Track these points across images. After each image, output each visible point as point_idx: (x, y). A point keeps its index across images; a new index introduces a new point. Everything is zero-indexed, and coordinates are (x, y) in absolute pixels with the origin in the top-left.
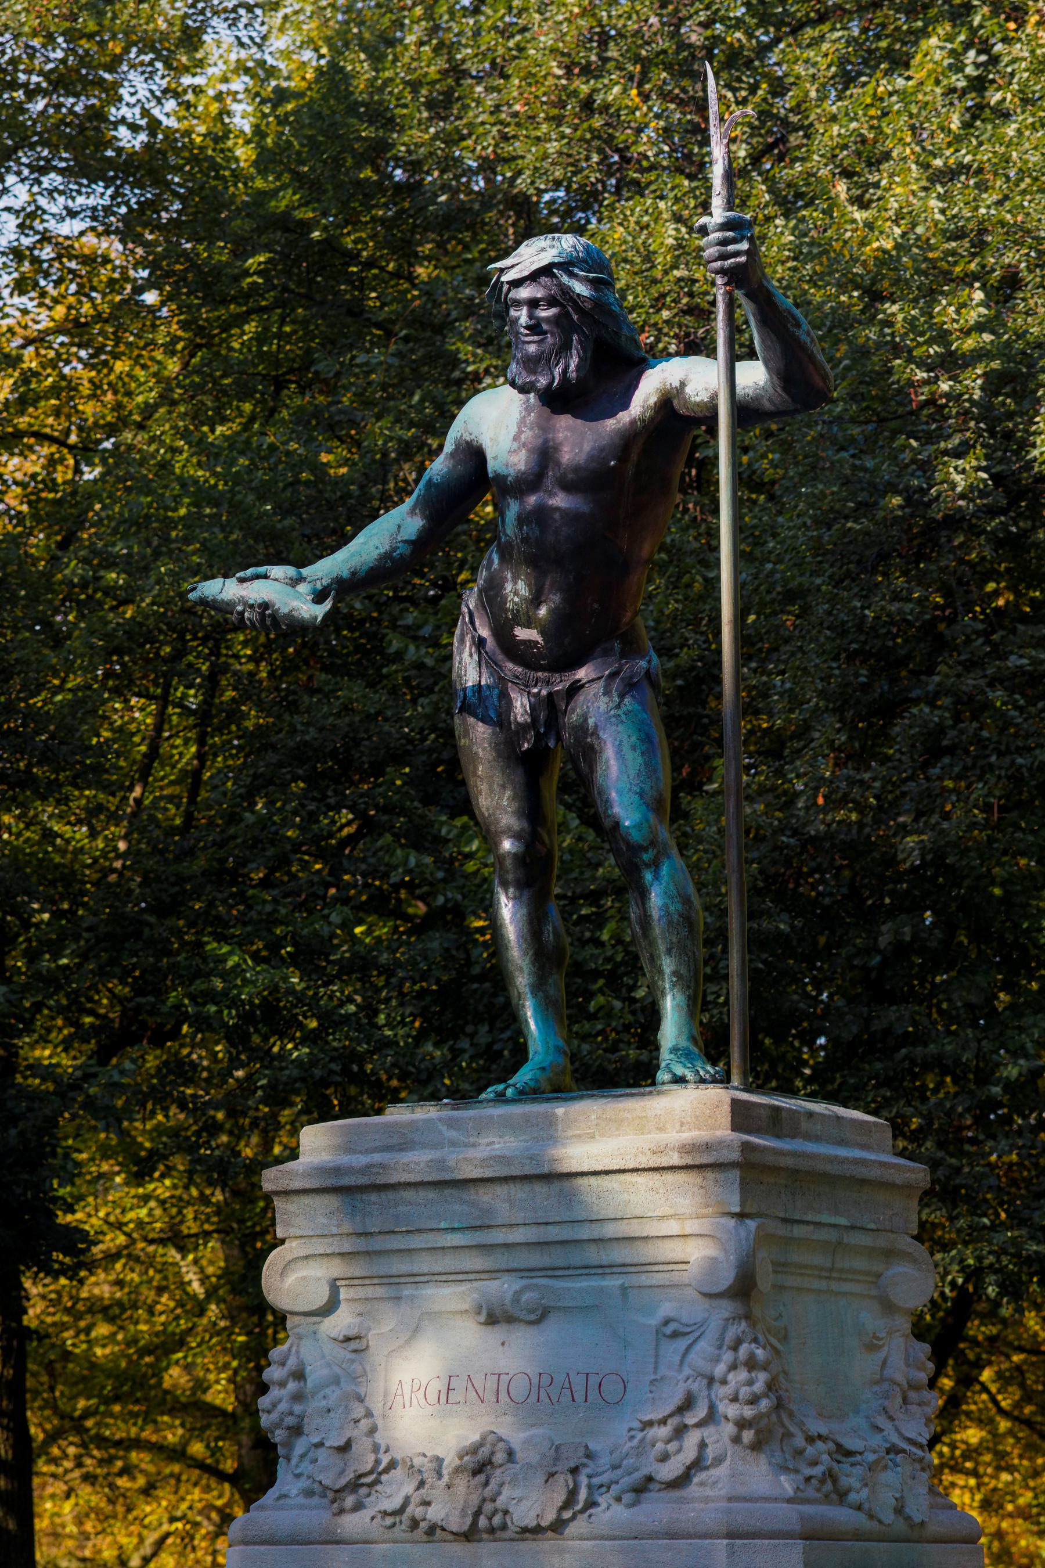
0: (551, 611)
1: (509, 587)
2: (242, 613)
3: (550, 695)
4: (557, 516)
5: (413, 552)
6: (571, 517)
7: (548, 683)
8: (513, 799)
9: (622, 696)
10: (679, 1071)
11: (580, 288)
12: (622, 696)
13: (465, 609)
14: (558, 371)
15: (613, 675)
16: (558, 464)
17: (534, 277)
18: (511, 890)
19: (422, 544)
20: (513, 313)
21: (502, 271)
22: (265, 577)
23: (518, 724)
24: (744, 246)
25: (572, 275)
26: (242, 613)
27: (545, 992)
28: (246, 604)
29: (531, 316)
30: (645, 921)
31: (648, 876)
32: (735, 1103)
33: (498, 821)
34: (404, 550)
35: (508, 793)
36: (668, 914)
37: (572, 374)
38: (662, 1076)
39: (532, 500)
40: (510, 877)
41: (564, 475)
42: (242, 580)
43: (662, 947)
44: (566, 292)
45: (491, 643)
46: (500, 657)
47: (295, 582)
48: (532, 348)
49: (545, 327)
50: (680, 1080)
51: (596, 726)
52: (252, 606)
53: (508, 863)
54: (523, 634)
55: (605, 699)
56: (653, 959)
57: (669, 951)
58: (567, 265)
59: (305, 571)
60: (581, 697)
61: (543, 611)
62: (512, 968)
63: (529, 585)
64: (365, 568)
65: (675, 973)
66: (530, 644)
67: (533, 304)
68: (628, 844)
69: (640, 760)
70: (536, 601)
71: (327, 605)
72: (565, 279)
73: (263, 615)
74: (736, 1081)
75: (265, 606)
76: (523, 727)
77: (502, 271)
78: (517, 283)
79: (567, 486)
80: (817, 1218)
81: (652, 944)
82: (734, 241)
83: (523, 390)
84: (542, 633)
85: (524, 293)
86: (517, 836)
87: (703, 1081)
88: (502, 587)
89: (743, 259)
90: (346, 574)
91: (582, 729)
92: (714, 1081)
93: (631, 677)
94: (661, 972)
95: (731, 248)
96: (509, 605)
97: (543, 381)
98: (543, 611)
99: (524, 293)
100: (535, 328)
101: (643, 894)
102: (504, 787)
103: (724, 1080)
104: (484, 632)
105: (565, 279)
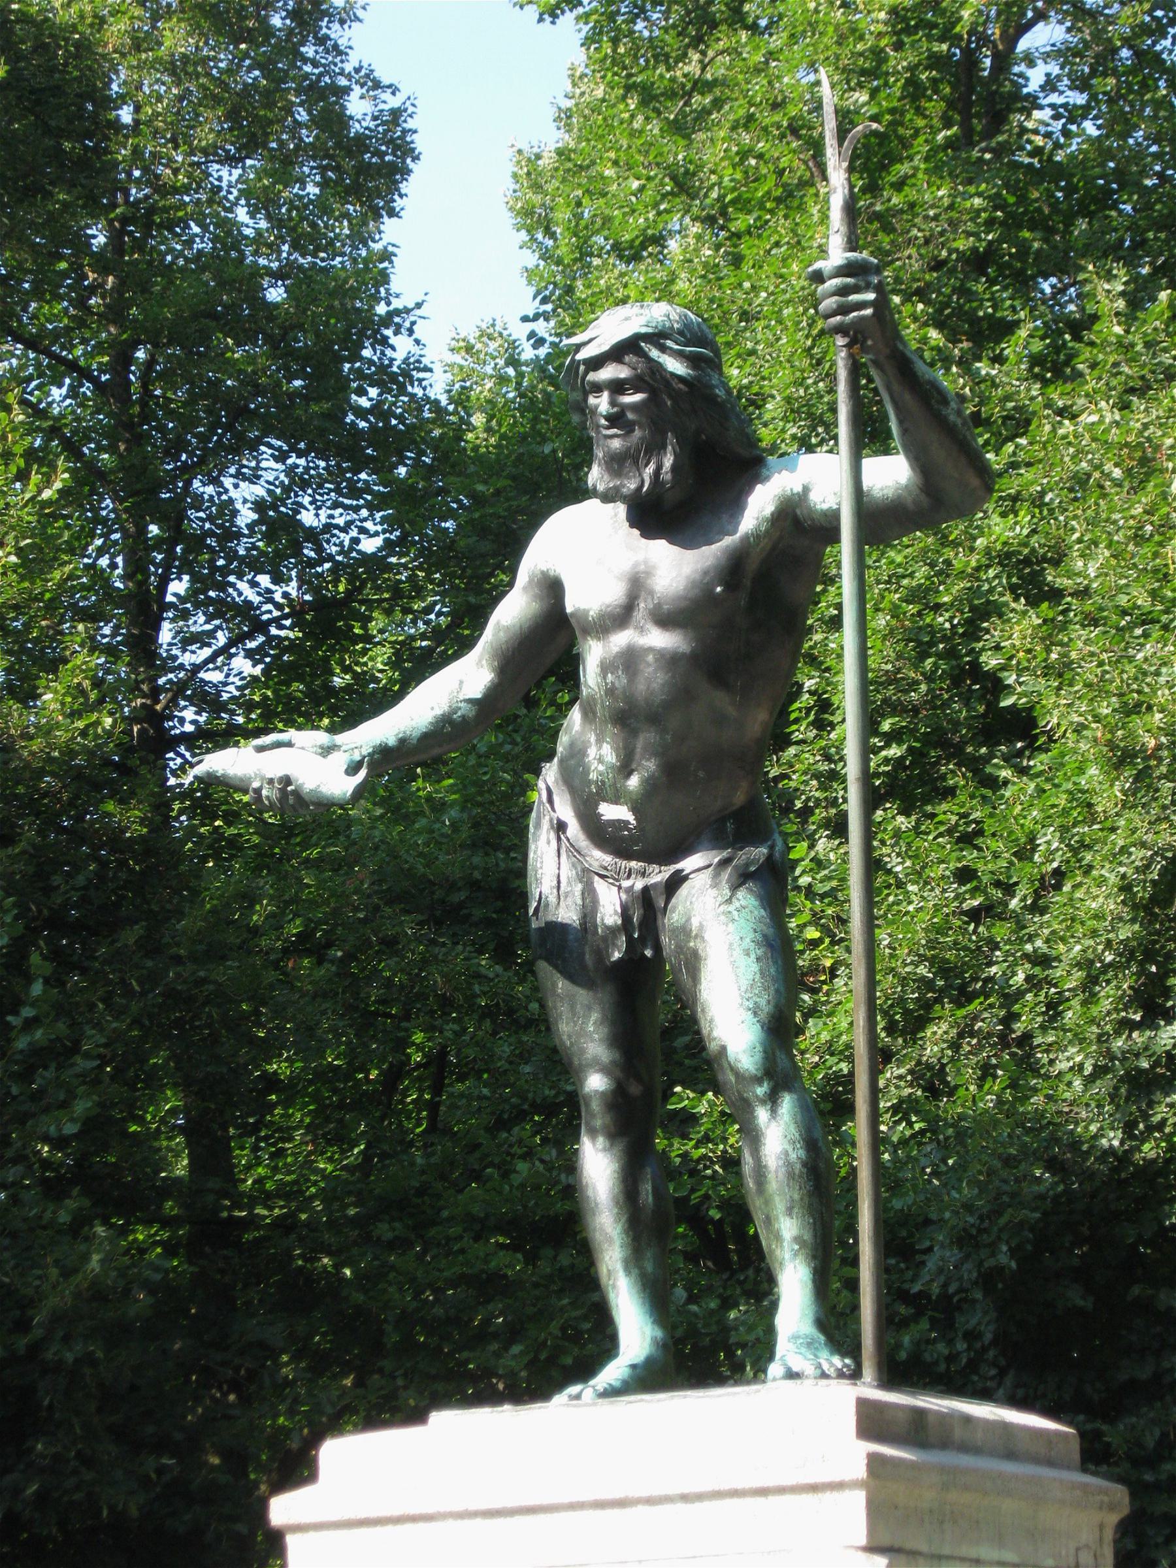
0: (645, 782)
1: (592, 752)
2: (258, 791)
3: (646, 889)
4: (650, 658)
5: (478, 716)
6: (670, 660)
7: (643, 874)
8: (598, 1024)
9: (735, 888)
10: (796, 1366)
11: (675, 366)
12: (735, 888)
13: (541, 784)
14: (650, 470)
15: (725, 863)
16: (651, 593)
17: (617, 353)
18: (601, 1141)
19: (486, 705)
20: (592, 400)
21: (578, 347)
22: (289, 744)
23: (607, 928)
24: (871, 296)
25: (663, 349)
26: (258, 791)
27: (641, 1268)
28: (263, 778)
29: (613, 403)
30: (760, 1171)
31: (762, 1114)
32: (863, 1405)
33: (583, 1051)
34: (465, 709)
35: (595, 1016)
36: (788, 1164)
37: (666, 475)
38: (775, 1369)
39: (621, 640)
40: (598, 1123)
41: (658, 606)
42: (261, 749)
43: (779, 1205)
44: (656, 369)
45: (574, 829)
46: (583, 842)
47: (326, 751)
48: (616, 444)
49: (630, 416)
50: (792, 1375)
51: (701, 927)
52: (271, 781)
53: (595, 1106)
54: (611, 812)
55: (714, 892)
56: (769, 1221)
57: (789, 1211)
58: (657, 337)
59: (340, 739)
60: (684, 891)
61: (634, 782)
62: (598, 1237)
63: (616, 750)
64: (416, 734)
65: (797, 1239)
66: (621, 824)
67: (617, 387)
68: (737, 1074)
69: (755, 967)
70: (626, 768)
71: (362, 774)
72: (654, 353)
73: (283, 791)
74: (868, 1374)
75: (287, 780)
76: (613, 931)
77: (578, 347)
78: (596, 363)
79: (665, 620)
80: (973, 1552)
81: (767, 1202)
82: (856, 289)
83: (608, 497)
84: (634, 810)
85: (607, 373)
86: (605, 1070)
87: (824, 1376)
88: (583, 753)
89: (869, 311)
90: (392, 741)
91: (684, 931)
92: (841, 1375)
93: (747, 865)
94: (778, 1237)
95: (854, 297)
96: (593, 776)
97: (632, 485)
98: (634, 782)
99: (607, 373)
100: (615, 420)
101: (752, 1135)
102: (589, 1008)
103: (855, 1375)
104: (565, 810)
105: (654, 353)
